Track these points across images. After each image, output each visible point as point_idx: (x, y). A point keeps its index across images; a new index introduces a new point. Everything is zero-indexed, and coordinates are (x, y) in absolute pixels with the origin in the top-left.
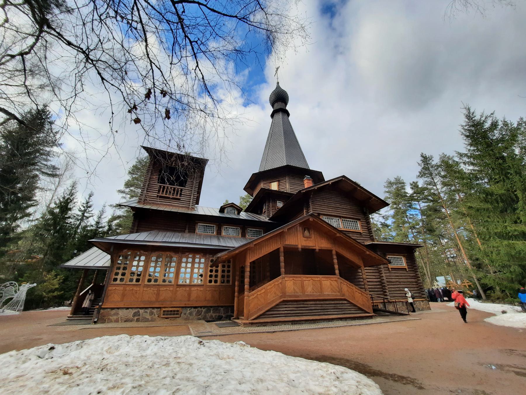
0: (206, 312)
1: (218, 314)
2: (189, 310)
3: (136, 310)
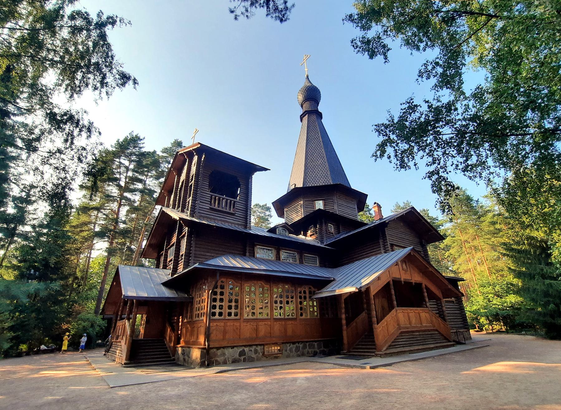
0: (305, 347)
1: (313, 350)
3: (241, 349)
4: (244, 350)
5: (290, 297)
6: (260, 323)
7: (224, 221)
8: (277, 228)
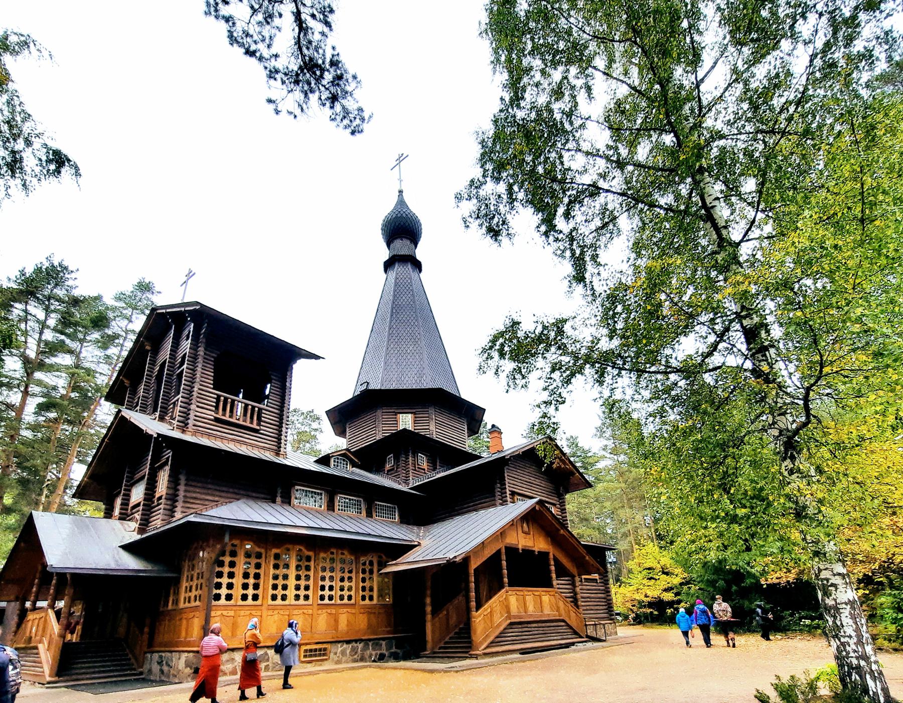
2: (341, 647)
4: (266, 654)
5: (346, 570)
6: (296, 612)
7: (239, 441)
8: (333, 456)
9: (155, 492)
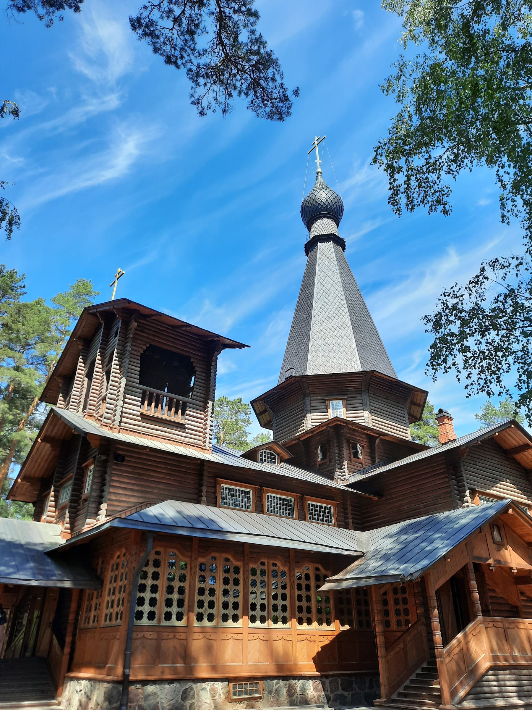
9: (81, 494)
